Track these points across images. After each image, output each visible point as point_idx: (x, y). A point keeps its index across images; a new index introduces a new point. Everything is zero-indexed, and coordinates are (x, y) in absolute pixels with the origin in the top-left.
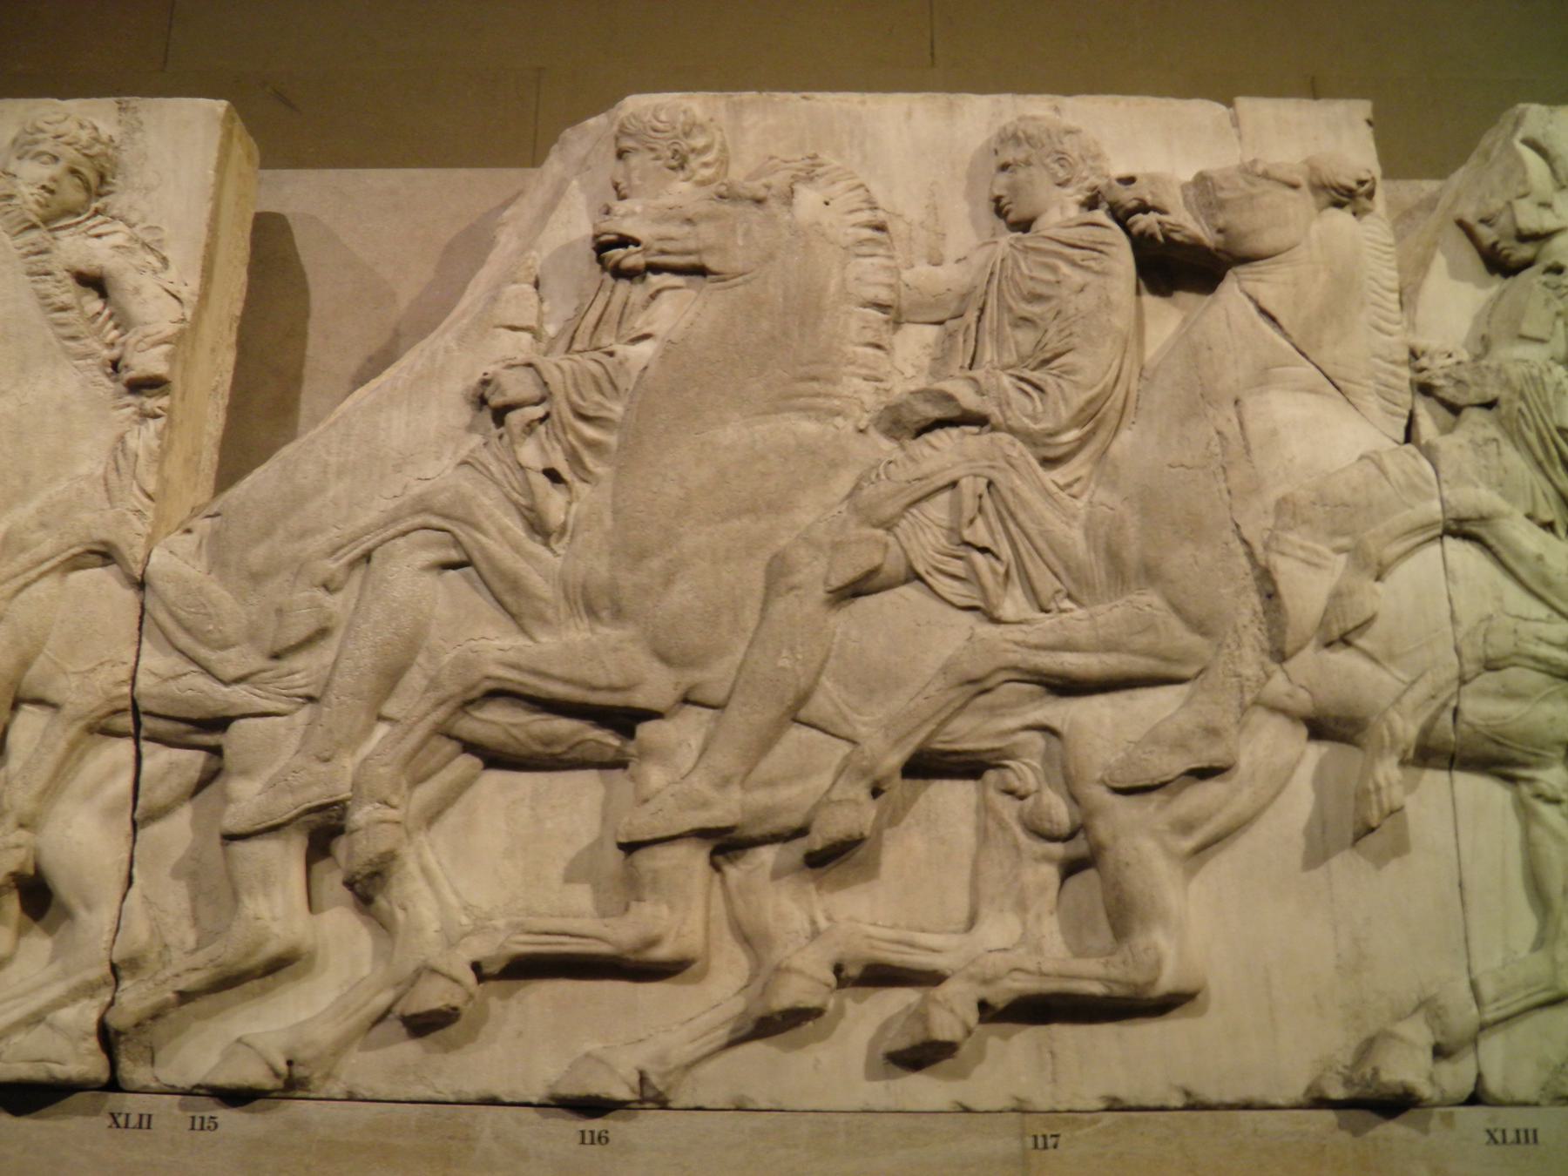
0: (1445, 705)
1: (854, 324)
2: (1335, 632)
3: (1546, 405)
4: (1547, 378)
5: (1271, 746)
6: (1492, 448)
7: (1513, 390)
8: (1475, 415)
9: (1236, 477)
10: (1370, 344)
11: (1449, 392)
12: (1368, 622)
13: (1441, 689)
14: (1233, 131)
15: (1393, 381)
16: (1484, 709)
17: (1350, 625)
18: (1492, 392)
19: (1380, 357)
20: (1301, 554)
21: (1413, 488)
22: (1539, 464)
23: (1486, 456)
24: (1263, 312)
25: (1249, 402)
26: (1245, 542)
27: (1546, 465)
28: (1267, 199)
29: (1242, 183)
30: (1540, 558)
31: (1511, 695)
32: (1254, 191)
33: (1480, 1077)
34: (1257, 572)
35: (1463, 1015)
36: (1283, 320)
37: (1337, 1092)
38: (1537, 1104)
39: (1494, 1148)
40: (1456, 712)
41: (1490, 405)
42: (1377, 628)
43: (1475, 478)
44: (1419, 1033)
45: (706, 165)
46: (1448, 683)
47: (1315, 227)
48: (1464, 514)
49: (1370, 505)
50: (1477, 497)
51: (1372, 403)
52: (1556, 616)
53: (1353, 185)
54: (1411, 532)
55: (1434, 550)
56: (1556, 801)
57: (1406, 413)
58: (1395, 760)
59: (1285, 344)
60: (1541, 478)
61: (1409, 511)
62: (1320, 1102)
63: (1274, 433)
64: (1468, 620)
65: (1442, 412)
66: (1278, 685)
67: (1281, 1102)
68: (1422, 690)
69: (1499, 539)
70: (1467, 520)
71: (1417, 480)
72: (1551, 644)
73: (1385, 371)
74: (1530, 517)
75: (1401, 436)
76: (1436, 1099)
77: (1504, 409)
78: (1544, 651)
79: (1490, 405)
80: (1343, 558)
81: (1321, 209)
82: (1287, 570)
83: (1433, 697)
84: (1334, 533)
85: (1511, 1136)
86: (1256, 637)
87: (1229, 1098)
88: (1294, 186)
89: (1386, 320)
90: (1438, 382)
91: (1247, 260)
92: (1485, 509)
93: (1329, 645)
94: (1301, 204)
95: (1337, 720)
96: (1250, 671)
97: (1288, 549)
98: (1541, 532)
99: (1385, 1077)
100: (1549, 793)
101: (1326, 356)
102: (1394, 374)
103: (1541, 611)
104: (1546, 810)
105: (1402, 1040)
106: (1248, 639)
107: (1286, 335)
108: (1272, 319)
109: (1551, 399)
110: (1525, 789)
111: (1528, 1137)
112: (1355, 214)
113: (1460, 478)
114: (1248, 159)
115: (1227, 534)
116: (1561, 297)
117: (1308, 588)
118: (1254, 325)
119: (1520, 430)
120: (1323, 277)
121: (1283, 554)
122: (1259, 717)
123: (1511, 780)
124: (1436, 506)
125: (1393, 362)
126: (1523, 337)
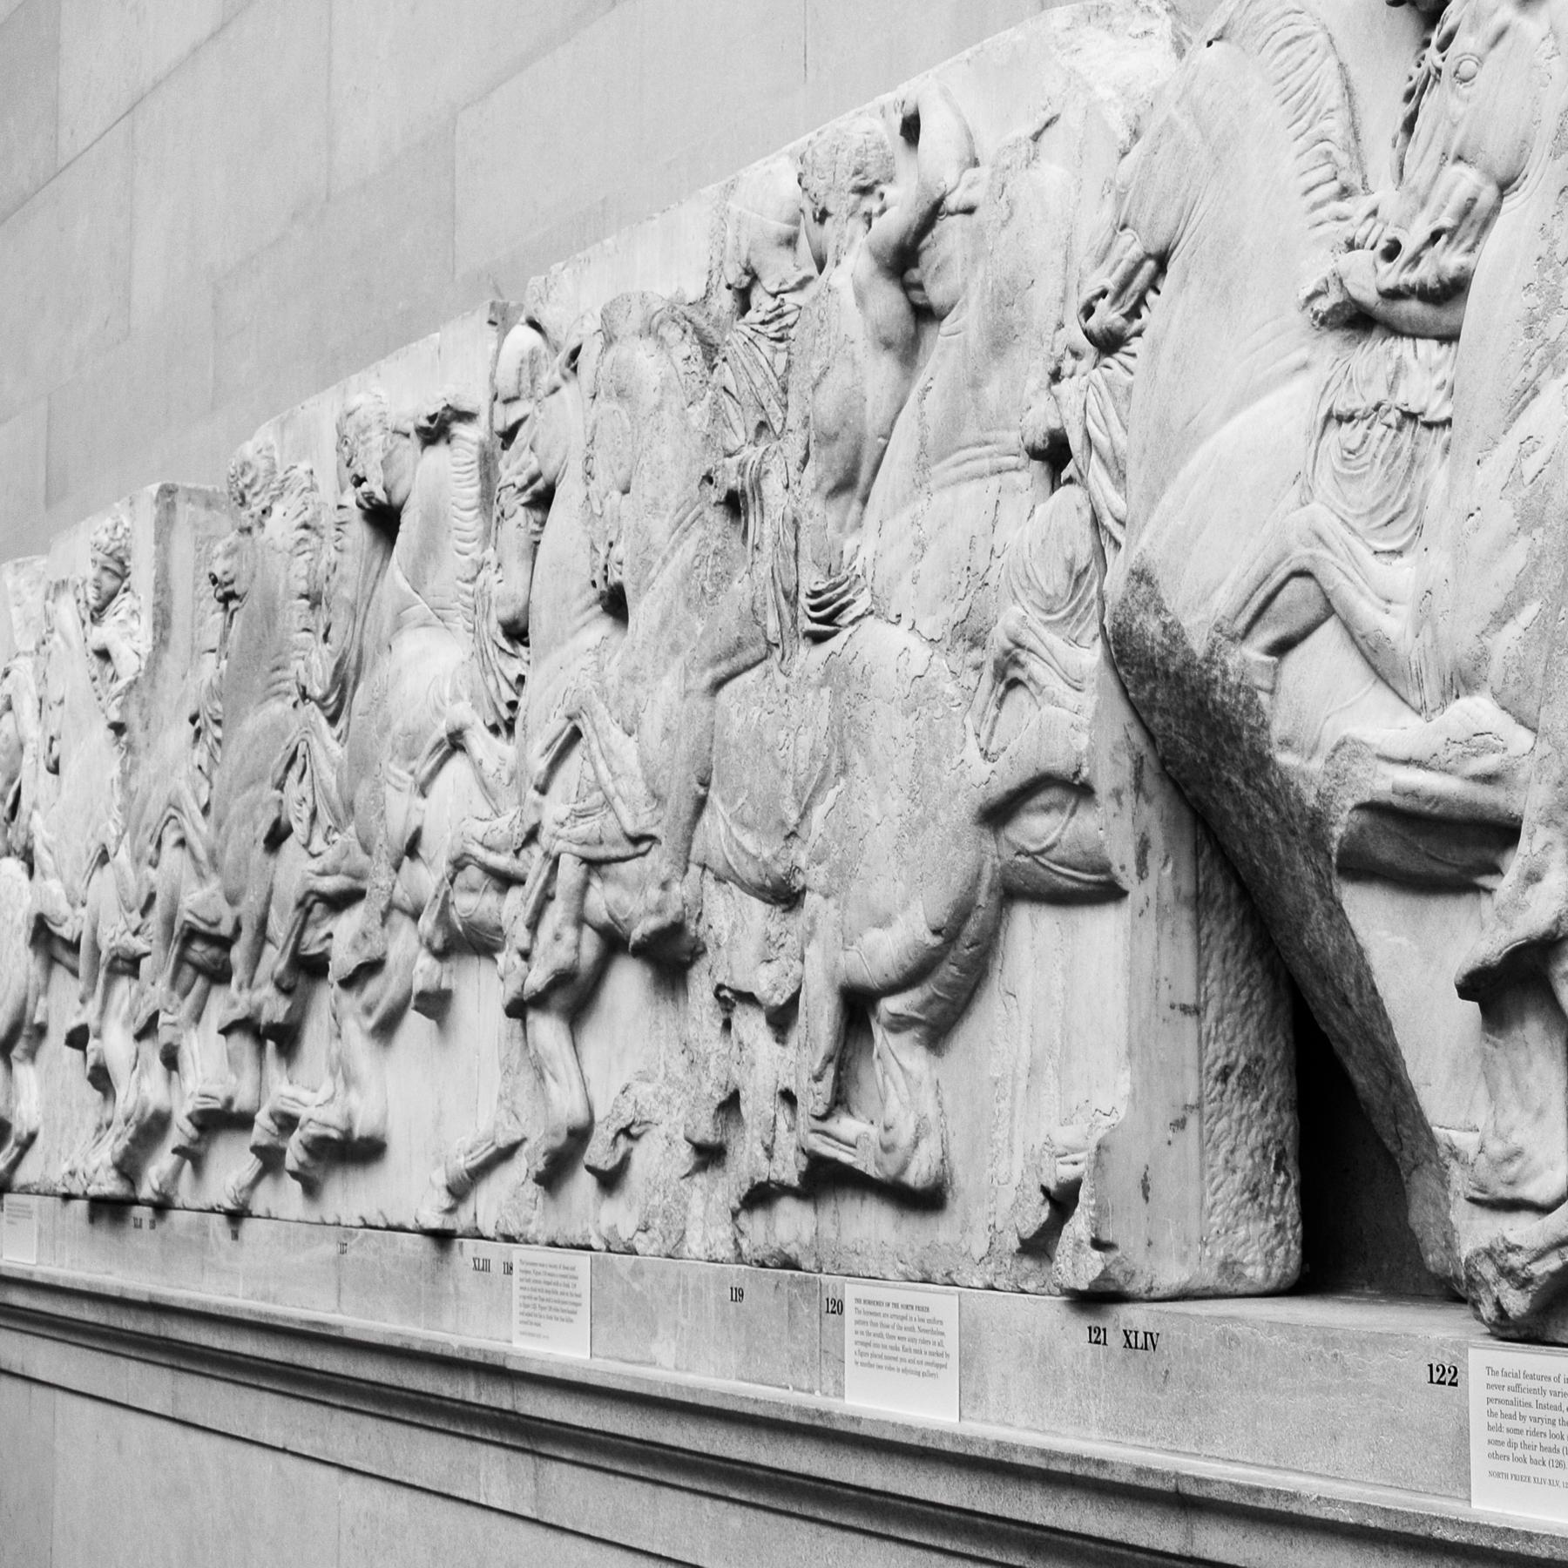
1: (295, 615)
45: (256, 494)
63: (400, 671)
88: (407, 435)
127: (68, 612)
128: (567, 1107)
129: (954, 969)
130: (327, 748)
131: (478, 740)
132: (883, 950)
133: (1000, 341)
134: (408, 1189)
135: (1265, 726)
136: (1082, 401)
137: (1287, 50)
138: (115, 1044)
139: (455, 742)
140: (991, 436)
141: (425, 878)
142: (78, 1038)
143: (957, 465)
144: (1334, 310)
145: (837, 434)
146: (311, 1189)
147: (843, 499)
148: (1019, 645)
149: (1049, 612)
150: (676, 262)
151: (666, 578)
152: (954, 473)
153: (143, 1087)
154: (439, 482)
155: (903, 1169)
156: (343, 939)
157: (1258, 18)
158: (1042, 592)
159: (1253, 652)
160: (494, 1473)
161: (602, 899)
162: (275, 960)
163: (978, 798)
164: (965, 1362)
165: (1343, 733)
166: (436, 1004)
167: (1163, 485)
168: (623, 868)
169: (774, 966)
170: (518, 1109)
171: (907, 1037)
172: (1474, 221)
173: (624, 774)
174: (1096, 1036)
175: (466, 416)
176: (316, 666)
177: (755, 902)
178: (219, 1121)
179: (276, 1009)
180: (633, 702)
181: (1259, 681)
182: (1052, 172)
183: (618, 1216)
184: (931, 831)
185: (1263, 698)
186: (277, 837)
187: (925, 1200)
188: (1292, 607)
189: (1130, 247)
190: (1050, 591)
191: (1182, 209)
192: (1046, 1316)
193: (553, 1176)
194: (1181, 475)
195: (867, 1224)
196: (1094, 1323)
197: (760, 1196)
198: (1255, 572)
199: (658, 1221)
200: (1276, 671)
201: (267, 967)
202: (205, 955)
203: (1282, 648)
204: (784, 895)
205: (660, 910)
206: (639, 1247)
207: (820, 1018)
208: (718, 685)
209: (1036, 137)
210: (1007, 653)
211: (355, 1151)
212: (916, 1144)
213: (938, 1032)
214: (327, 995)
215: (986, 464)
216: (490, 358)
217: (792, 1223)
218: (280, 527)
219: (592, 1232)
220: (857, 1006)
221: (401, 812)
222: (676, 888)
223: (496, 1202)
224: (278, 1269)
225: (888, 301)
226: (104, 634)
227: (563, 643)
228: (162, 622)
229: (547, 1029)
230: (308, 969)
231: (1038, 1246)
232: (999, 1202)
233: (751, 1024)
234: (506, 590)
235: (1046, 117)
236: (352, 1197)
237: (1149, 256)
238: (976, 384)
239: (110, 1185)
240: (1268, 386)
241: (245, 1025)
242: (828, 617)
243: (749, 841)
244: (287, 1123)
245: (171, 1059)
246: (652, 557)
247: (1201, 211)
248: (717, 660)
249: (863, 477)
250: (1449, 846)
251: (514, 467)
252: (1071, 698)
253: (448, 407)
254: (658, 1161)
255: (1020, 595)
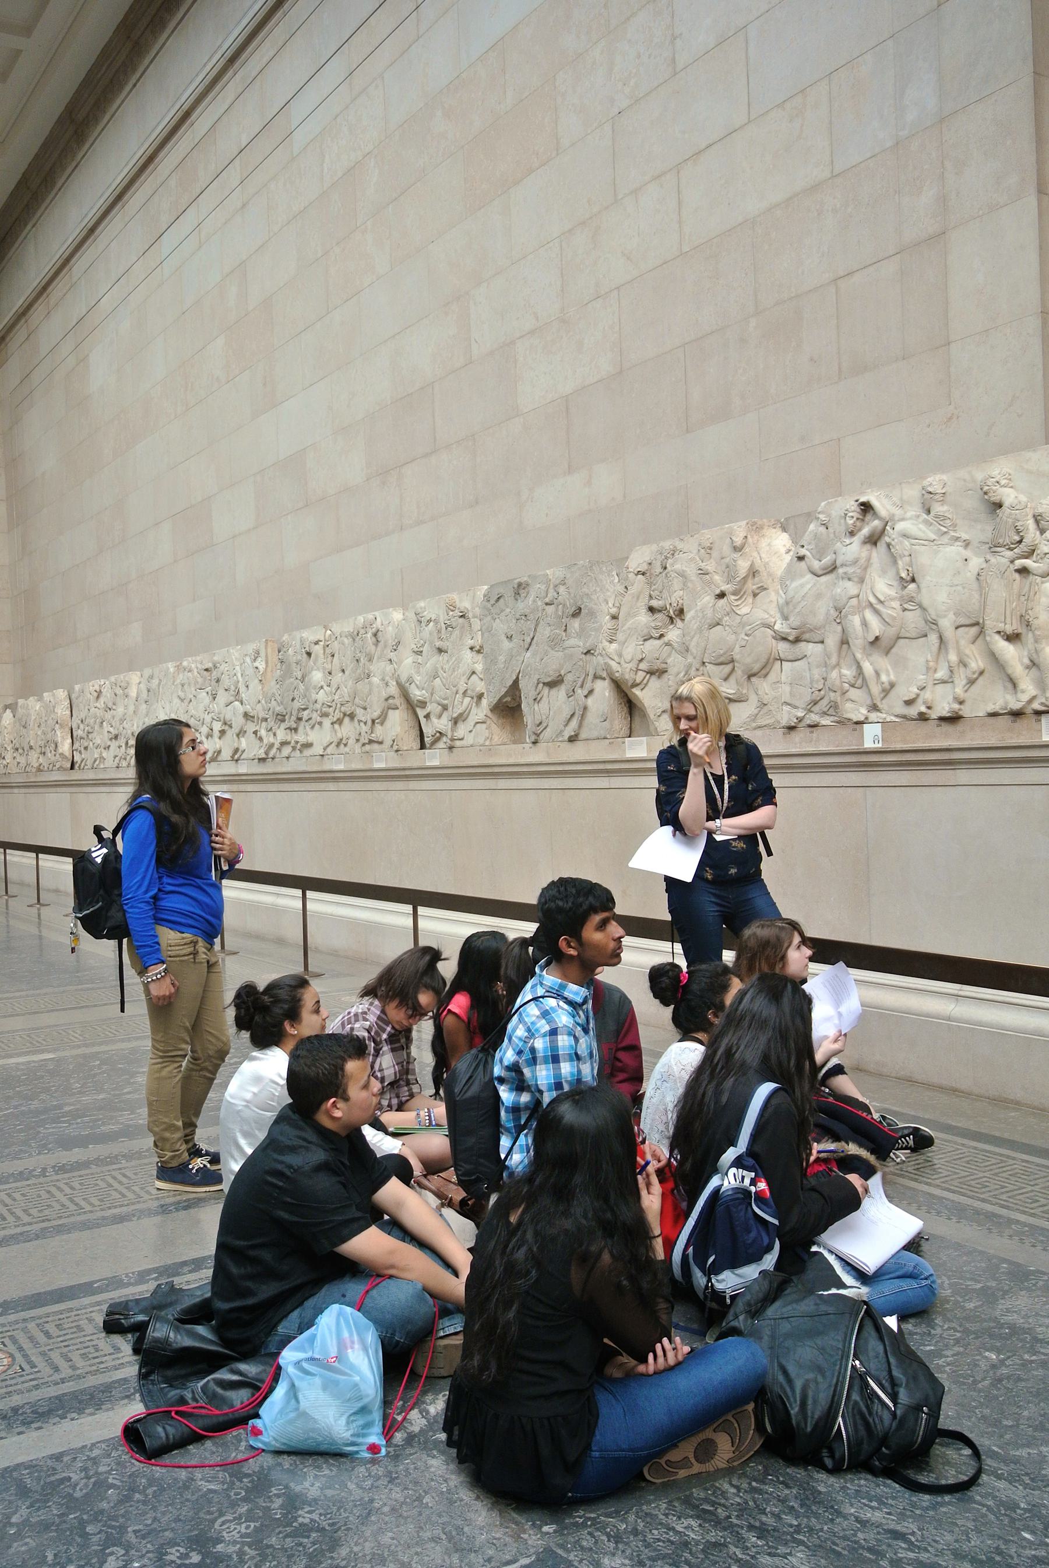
127: (248, 659)
128: (339, 735)
130: (302, 687)
131: (325, 688)
132: (376, 714)
133: (385, 646)
134: (318, 750)
136: (392, 655)
138: (263, 733)
139: (322, 687)
141: (318, 706)
142: (255, 733)
146: (301, 752)
150: (348, 627)
151: (349, 669)
153: (268, 739)
154: (318, 650)
156: (305, 715)
160: (331, 786)
161: (343, 709)
162: (294, 718)
165: (416, 693)
166: (320, 723)
172: (423, 646)
173: (345, 691)
174: (397, 723)
176: (299, 675)
178: (284, 744)
179: (294, 726)
180: (345, 684)
182: (390, 628)
183: (347, 749)
186: (293, 700)
187: (381, 743)
188: (410, 680)
192: (393, 753)
193: (338, 745)
195: (376, 746)
197: (364, 745)
201: (292, 718)
202: (281, 718)
204: (365, 709)
207: (369, 723)
211: (308, 745)
213: (382, 724)
214: (302, 723)
217: (367, 747)
218: (291, 652)
220: (373, 721)
221: (314, 696)
223: (329, 751)
224: (297, 764)
225: (374, 639)
226: (256, 664)
228: (267, 663)
229: (336, 726)
230: (300, 719)
231: (392, 746)
232: (388, 742)
233: (362, 724)
234: (328, 666)
236: (308, 752)
239: (264, 756)
241: (290, 729)
242: (369, 676)
244: (297, 742)
245: (275, 735)
250: (423, 704)
251: (328, 651)
254: (351, 742)
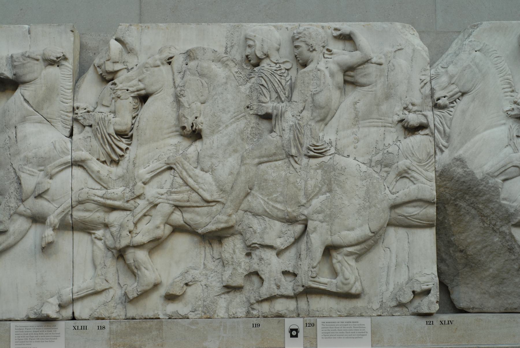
0: (67, 214)
2: (37, 193)
3: (105, 127)
4: (106, 119)
5: (19, 225)
6: (89, 140)
7: (95, 122)
8: (87, 128)
9: (12, 150)
10: (61, 107)
11: (82, 121)
12: (48, 190)
13: (65, 209)
14: (29, 36)
15: (66, 118)
16: (79, 214)
17: (41, 192)
18: (92, 122)
19: (63, 111)
20: (28, 172)
21: (63, 152)
22: (101, 144)
23: (87, 142)
24: (25, 99)
25: (19, 127)
26: (14, 169)
27: (103, 145)
28: (28, 64)
29: (21, 60)
30: (98, 172)
31: (87, 210)
32: (25, 62)
33: (73, 313)
34: (16, 178)
35: (67, 296)
36: (31, 102)
37: (32, 316)
38: (88, 320)
39: (75, 330)
40: (72, 215)
41: (91, 126)
42: (50, 192)
43: (83, 149)
44: (55, 301)
46: (68, 208)
47: (44, 72)
48: (77, 159)
49: (50, 158)
50: (83, 154)
51: (60, 125)
52: (103, 188)
53: (55, 59)
54: (61, 165)
55: (70, 169)
56: (100, 239)
57: (70, 127)
58: (51, 229)
59: (31, 109)
60: (102, 148)
61: (62, 159)
62: (29, 320)
63: (25, 136)
64: (75, 189)
65: (80, 127)
66: (22, 208)
67: (19, 319)
68: (60, 209)
69: (88, 167)
70: (78, 161)
71: (65, 150)
72: (98, 196)
73: (64, 115)
74: (98, 159)
75: (68, 134)
76: (61, 318)
77: (93, 127)
78: (96, 198)
79: (91, 126)
80: (42, 173)
81: (46, 67)
82: (23, 176)
83: (63, 212)
84: (39, 166)
85: (80, 328)
86: (15, 195)
87: (4, 318)
88: (37, 60)
89: (66, 99)
90: (79, 118)
91: (24, 83)
92: (83, 158)
93: (35, 197)
94: (39, 66)
95: (38, 217)
96: (12, 205)
97: (25, 171)
98: (101, 164)
99: (43, 312)
100: (98, 237)
101: (43, 112)
102: (67, 116)
103: (99, 187)
104: (97, 242)
105: (49, 303)
106: (13, 196)
107: (32, 107)
108: (28, 102)
109: (107, 125)
110: (93, 236)
111: (84, 328)
112: (58, 66)
113: (78, 149)
114: (24, 51)
115: (9, 167)
116: (114, 93)
117: (29, 182)
118: (22, 104)
119: (96, 134)
120: (44, 88)
121: (23, 172)
122: (16, 217)
123: (90, 234)
124: (70, 157)
125: (67, 112)
126: (103, 105)
129: (373, 241)
135: (499, 195)
137: (496, 59)
140: (383, 118)
143: (369, 122)
144: (515, 115)
145: (324, 107)
147: (321, 123)
148: (409, 169)
149: (420, 163)
152: (368, 124)
155: (351, 289)
157: (488, 50)
158: (418, 158)
159: (499, 180)
163: (391, 202)
164: (373, 333)
167: (466, 142)
168: (197, 209)
169: (282, 239)
170: (107, 279)
171: (351, 258)
175: (65, 58)
177: (276, 222)
181: (500, 186)
184: (373, 209)
185: (500, 189)
189: (454, 89)
190: (420, 158)
191: (473, 85)
194: (472, 140)
196: (428, 320)
198: (502, 163)
199: (200, 309)
200: (503, 185)
203: (505, 180)
205: (226, 222)
206: (190, 316)
208: (260, 163)
209: (395, 51)
210: (405, 170)
212: (355, 283)
215: (380, 124)
216: (72, 42)
219: (160, 313)
222: (234, 216)
227: (158, 141)
235: (399, 48)
237: (460, 92)
238: (378, 105)
240: (496, 126)
243: (279, 206)
246: (221, 124)
247: (479, 86)
248: (259, 157)
249: (328, 119)
252: (428, 183)
253: (64, 55)
255: (409, 158)
